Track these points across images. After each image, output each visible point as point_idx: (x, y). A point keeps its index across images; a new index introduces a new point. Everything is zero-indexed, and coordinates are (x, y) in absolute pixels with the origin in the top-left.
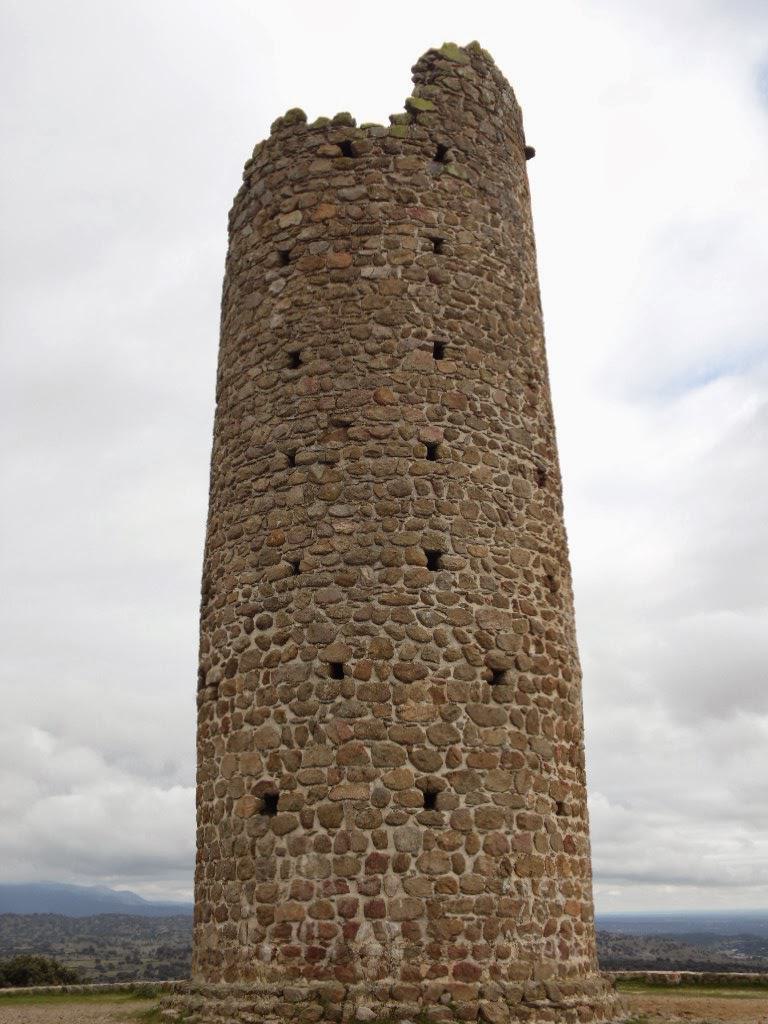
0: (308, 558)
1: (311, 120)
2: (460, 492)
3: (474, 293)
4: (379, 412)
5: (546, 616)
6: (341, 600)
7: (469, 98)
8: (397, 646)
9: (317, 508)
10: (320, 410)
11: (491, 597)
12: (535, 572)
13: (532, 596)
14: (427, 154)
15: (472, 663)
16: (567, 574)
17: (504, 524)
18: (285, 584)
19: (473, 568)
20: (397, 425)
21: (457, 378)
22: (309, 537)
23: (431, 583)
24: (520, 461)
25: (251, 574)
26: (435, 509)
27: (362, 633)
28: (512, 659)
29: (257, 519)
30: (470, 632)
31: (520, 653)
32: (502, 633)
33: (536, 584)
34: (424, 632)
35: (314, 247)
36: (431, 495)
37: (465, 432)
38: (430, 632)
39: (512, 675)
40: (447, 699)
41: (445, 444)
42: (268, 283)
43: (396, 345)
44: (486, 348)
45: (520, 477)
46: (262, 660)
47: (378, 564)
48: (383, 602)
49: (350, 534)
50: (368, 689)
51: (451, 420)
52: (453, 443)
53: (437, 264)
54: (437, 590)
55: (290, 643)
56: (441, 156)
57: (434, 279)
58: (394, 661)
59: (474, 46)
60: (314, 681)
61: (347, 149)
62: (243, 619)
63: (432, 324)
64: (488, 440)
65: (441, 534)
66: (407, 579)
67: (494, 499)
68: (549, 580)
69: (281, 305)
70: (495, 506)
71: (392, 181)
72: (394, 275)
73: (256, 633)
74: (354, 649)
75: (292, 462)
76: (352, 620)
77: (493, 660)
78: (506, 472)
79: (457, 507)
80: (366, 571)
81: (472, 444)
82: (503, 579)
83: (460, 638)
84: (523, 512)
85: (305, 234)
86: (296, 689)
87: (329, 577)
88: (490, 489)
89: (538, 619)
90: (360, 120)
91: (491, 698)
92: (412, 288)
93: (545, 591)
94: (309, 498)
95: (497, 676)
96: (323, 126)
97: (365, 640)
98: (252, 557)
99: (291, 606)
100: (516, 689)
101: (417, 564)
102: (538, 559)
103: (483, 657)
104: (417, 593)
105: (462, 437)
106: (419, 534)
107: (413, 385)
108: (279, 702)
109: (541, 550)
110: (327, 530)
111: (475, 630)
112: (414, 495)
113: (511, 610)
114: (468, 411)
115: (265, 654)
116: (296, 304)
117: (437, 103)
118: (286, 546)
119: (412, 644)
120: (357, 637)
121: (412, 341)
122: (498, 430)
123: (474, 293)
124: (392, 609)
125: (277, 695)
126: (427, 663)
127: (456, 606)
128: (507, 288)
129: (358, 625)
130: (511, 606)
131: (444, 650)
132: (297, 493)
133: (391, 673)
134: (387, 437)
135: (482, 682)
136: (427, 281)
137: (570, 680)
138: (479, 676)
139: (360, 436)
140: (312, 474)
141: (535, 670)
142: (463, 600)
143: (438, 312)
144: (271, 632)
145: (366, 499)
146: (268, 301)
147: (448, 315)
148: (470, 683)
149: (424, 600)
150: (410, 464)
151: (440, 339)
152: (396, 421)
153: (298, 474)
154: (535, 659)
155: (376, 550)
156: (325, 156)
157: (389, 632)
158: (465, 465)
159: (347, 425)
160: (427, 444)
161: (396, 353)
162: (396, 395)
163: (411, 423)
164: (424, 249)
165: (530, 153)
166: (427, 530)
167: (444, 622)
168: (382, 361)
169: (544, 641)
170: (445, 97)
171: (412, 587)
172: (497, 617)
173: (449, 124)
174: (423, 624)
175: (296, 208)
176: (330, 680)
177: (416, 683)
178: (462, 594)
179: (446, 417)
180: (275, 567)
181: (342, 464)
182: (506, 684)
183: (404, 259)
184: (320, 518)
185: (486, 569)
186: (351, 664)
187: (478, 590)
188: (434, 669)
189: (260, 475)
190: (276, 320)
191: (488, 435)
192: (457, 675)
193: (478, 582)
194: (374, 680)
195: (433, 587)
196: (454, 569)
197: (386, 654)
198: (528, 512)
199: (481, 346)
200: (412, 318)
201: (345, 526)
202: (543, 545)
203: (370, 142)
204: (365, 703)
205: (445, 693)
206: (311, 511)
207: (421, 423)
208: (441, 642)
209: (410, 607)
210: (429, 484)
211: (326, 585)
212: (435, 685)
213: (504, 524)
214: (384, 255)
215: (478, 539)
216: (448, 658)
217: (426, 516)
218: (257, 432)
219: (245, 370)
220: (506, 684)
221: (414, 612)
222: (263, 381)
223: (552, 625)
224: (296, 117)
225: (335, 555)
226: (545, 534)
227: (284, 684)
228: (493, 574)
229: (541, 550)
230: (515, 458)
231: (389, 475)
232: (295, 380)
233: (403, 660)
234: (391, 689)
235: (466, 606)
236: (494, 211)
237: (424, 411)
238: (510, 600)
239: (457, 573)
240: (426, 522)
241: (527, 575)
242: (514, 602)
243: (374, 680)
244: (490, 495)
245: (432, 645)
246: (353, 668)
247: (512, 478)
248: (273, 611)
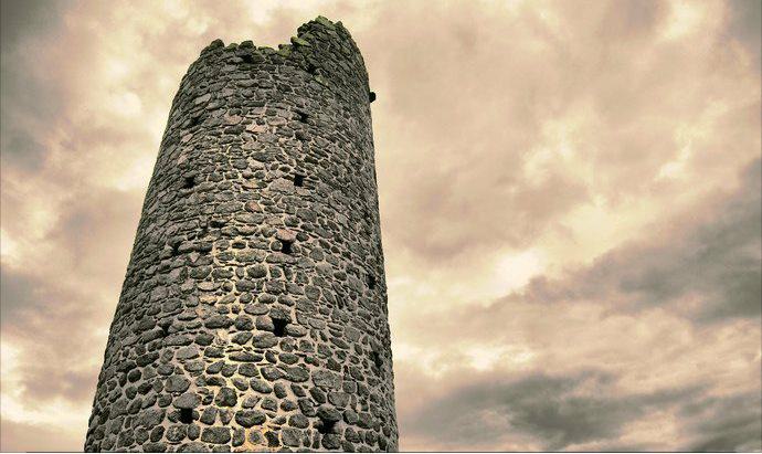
0: (176, 322)
1: (227, 45)
2: (306, 278)
3: (328, 151)
4: (248, 216)
5: (371, 382)
6: (197, 356)
7: (333, 47)
8: (241, 395)
9: (188, 285)
10: (202, 214)
11: (326, 361)
12: (363, 347)
13: (360, 365)
14: (302, 68)
15: (306, 413)
16: (389, 355)
17: (341, 307)
18: (155, 344)
19: (312, 337)
20: (260, 227)
21: (310, 200)
22: (180, 306)
23: (275, 345)
24: (355, 266)
25: (132, 338)
26: (284, 288)
27: (212, 382)
28: (341, 412)
29: (144, 295)
30: (306, 388)
31: (348, 408)
32: (333, 390)
33: (364, 356)
34: (265, 385)
35: (215, 114)
36: (283, 278)
37: (315, 237)
38: (271, 385)
39: (342, 426)
40: (281, 443)
41: (297, 243)
42: (180, 138)
43: (266, 174)
44: (335, 187)
45: (355, 276)
46: (128, 407)
47: (232, 328)
48: (232, 358)
49: (212, 304)
50: (211, 431)
51: (303, 227)
52: (304, 243)
53: (303, 128)
54: (281, 352)
55: (152, 392)
56: (311, 70)
57: (299, 137)
58: (238, 408)
59: (340, 24)
60: (166, 424)
61: (247, 59)
62: (120, 374)
63: (295, 163)
64: (332, 246)
65: (287, 308)
66: (255, 341)
67: (333, 288)
68: (374, 355)
69: (186, 149)
70: (333, 293)
71: (276, 78)
72: (270, 130)
73: (128, 385)
74: (203, 397)
75: (175, 253)
76: (204, 373)
77: (324, 412)
78: (344, 271)
79: (303, 289)
80: (222, 334)
81: (318, 246)
82: (337, 349)
83: (298, 392)
84: (356, 302)
85: (211, 106)
86: (150, 432)
87: (191, 337)
88: (330, 280)
89: (365, 383)
90: (258, 44)
91: (321, 445)
92: (282, 140)
93: (371, 363)
94: (184, 276)
95: (327, 426)
96: (233, 48)
97: (216, 390)
98: (136, 324)
99: (157, 362)
100: (343, 438)
101: (265, 330)
102: (366, 338)
103: (316, 409)
104: (262, 352)
105: (311, 240)
106: (269, 306)
107: (276, 201)
108: (135, 444)
109: (369, 332)
110: (194, 300)
111: (310, 384)
112: (269, 276)
113: (342, 374)
114: (317, 223)
115: (131, 402)
116: (197, 147)
117: (312, 43)
118: (161, 314)
119: (255, 394)
120: (208, 387)
121: (279, 173)
122: (341, 241)
123: (328, 151)
124: (240, 364)
125: (134, 437)
126: (267, 411)
127: (295, 365)
128: (352, 155)
129: (208, 376)
130: (343, 370)
131: (282, 401)
132: (176, 273)
133: (233, 419)
134: (251, 234)
135: (314, 430)
136: (294, 137)
137: (389, 436)
138: (311, 424)
139: (229, 232)
140: (189, 259)
141: (360, 424)
142: (301, 361)
143: (300, 157)
144: (137, 385)
145: (229, 278)
146: (180, 148)
147: (307, 160)
148: (303, 430)
149: (268, 358)
150: (268, 254)
151: (299, 173)
152: (260, 223)
153: (179, 260)
154: (361, 415)
155: (232, 316)
156: (232, 63)
157: (236, 383)
158: (312, 260)
159: (222, 225)
160: (283, 241)
161: (265, 179)
162: (263, 207)
163: (271, 226)
164: (293, 119)
165: (372, 97)
166: (276, 303)
167: (284, 377)
168: (253, 183)
169: (369, 402)
170: (318, 42)
171: (258, 347)
172: (330, 377)
173: (318, 55)
174: (266, 377)
175: (208, 92)
176: (179, 423)
177: (254, 428)
178: (301, 356)
179: (299, 225)
180: (150, 331)
181: (214, 253)
182: (335, 433)
183: (278, 123)
184: (189, 292)
185: (324, 339)
186: (199, 409)
187: (314, 354)
188: (272, 417)
189: (150, 264)
190: (183, 159)
191: (332, 242)
192: (292, 423)
193: (316, 348)
194: (218, 424)
195: (277, 348)
196: (296, 336)
197: (230, 401)
198: (360, 303)
199: (330, 184)
200: (280, 158)
201: (209, 298)
202: (371, 329)
203: (264, 56)
204: (208, 444)
205: (280, 438)
206: (183, 287)
207: (280, 226)
208: (280, 394)
209: (255, 364)
210: (281, 270)
211: (188, 343)
212: (271, 430)
213: (341, 307)
214: (265, 119)
215: (318, 315)
216: (286, 408)
217: (276, 293)
218: (155, 234)
219: (156, 194)
220: (335, 433)
221: (259, 368)
222: (165, 200)
223: (375, 391)
224: (219, 44)
225: (199, 320)
226: (372, 321)
227: (141, 427)
228: (329, 344)
229: (369, 332)
230: (352, 262)
231: (249, 261)
232: (187, 196)
233: (245, 407)
234: (232, 432)
235: (304, 365)
236: (345, 109)
237: (282, 219)
238: (342, 366)
239: (299, 339)
240: (277, 298)
241: (358, 350)
242: (346, 367)
243: (218, 424)
244: (330, 284)
245: (272, 396)
246: (201, 414)
247: (348, 276)
248: (143, 366)
